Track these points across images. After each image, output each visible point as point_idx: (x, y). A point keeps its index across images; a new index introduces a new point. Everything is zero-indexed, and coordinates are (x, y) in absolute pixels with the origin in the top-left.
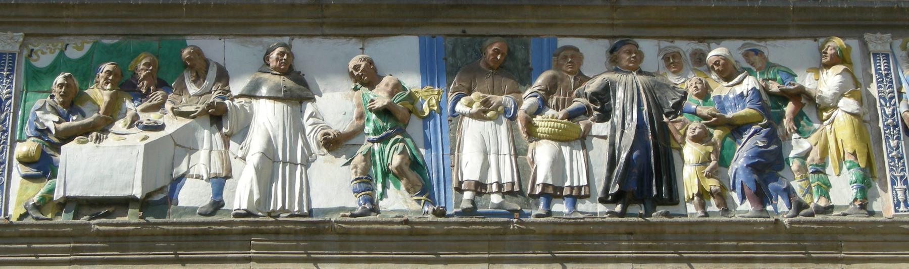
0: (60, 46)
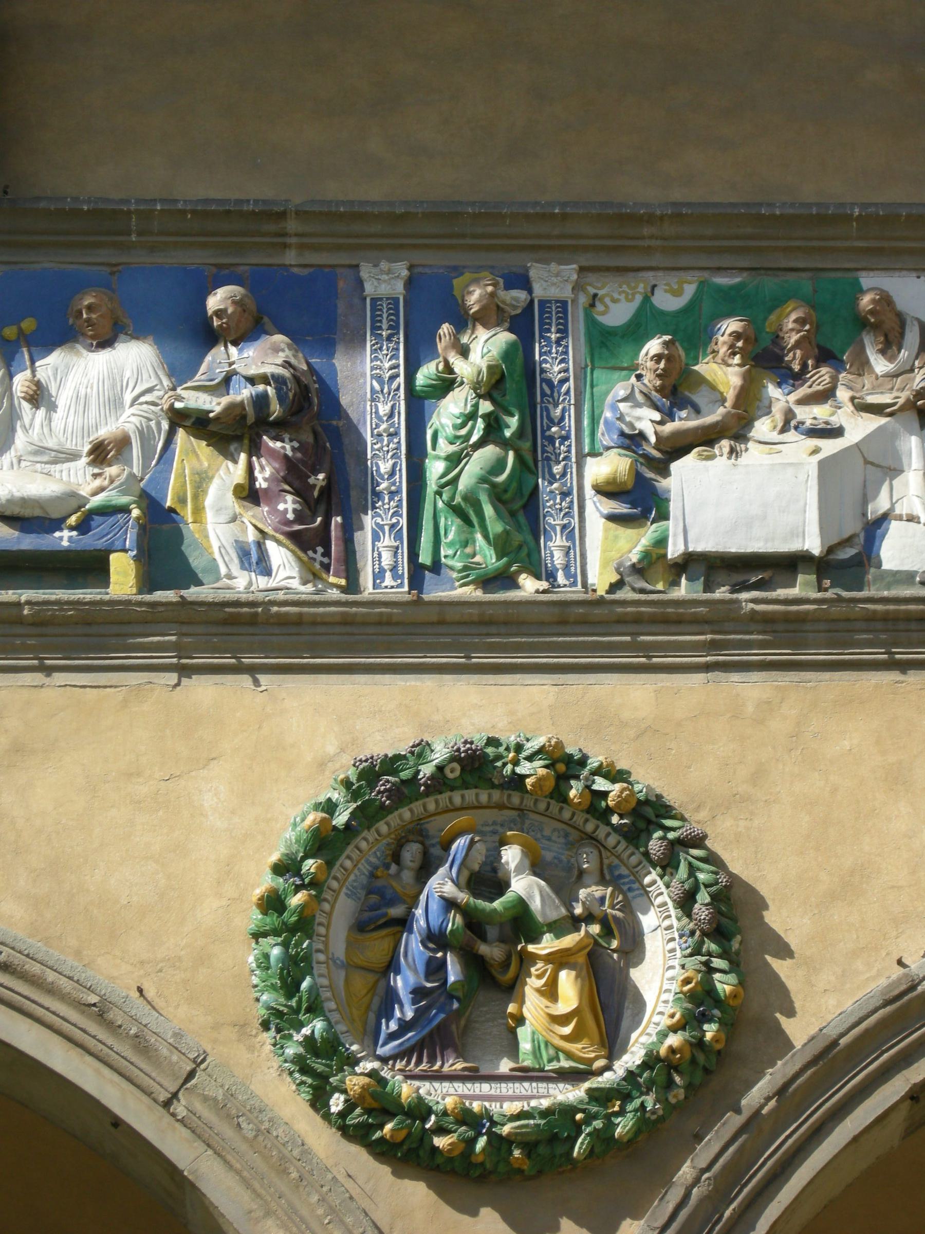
0: (641, 288)
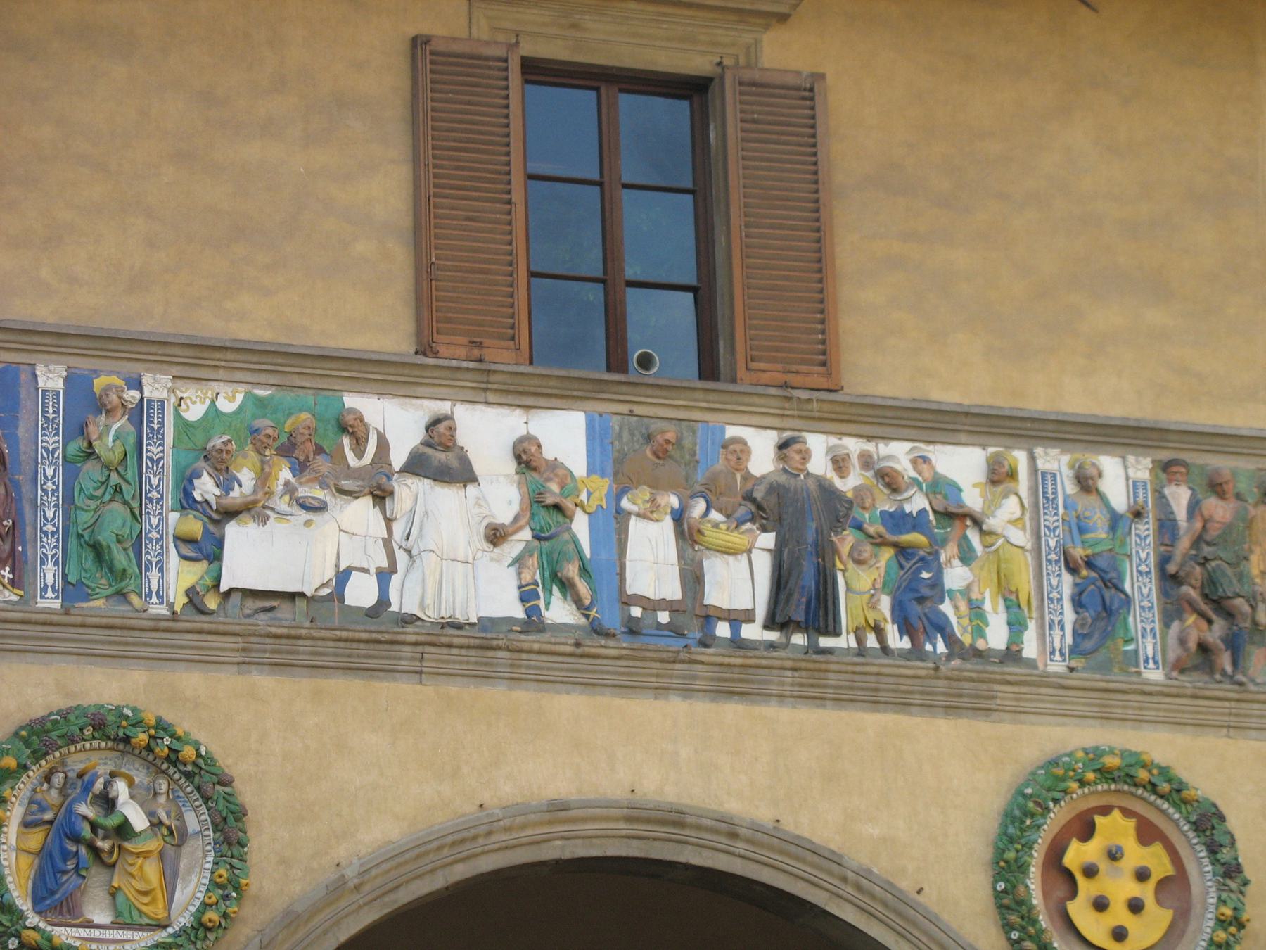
0: (209, 394)
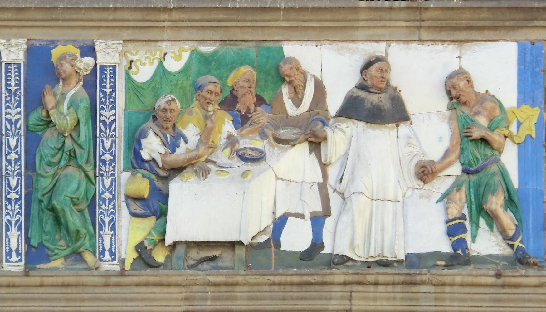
0: (158, 55)
